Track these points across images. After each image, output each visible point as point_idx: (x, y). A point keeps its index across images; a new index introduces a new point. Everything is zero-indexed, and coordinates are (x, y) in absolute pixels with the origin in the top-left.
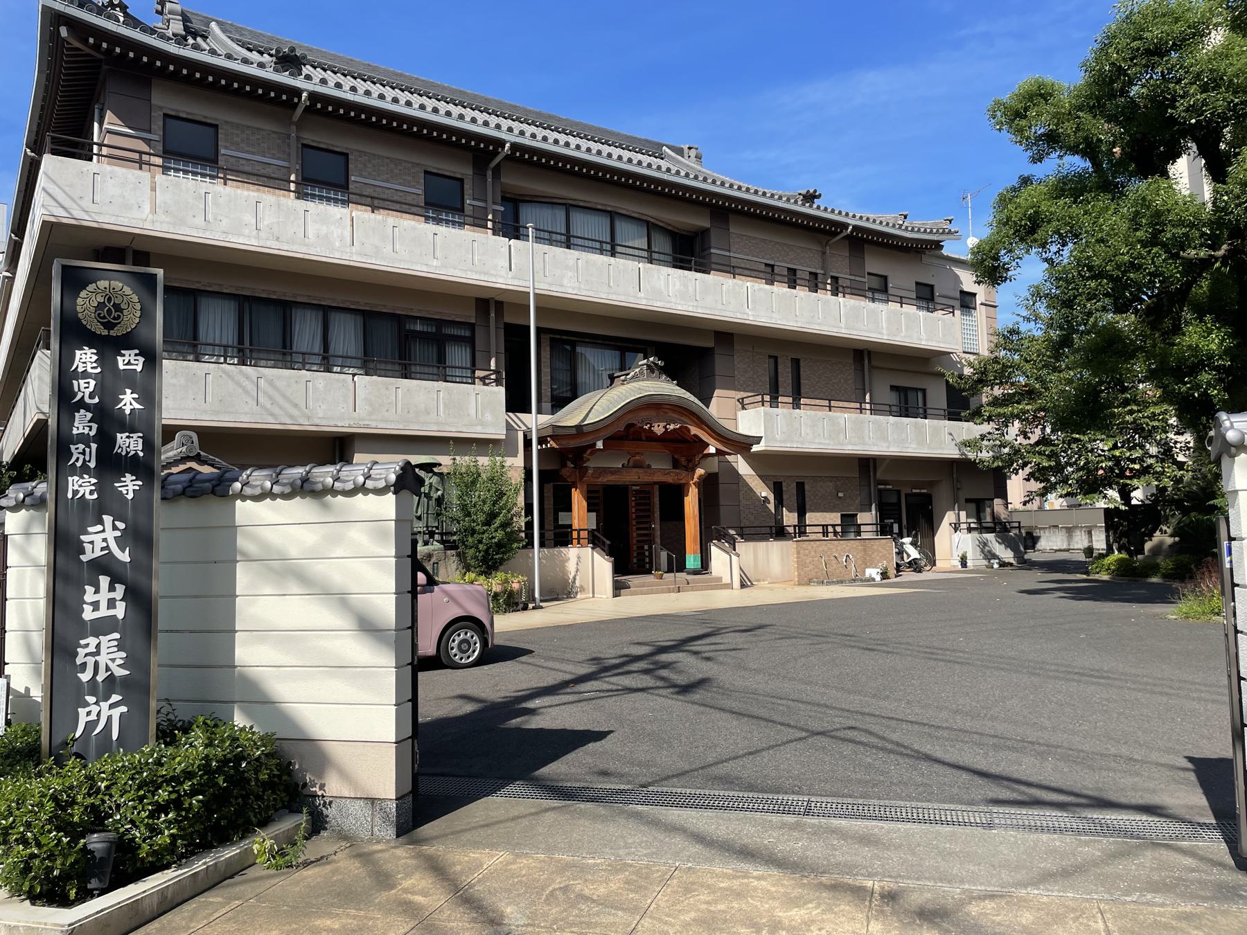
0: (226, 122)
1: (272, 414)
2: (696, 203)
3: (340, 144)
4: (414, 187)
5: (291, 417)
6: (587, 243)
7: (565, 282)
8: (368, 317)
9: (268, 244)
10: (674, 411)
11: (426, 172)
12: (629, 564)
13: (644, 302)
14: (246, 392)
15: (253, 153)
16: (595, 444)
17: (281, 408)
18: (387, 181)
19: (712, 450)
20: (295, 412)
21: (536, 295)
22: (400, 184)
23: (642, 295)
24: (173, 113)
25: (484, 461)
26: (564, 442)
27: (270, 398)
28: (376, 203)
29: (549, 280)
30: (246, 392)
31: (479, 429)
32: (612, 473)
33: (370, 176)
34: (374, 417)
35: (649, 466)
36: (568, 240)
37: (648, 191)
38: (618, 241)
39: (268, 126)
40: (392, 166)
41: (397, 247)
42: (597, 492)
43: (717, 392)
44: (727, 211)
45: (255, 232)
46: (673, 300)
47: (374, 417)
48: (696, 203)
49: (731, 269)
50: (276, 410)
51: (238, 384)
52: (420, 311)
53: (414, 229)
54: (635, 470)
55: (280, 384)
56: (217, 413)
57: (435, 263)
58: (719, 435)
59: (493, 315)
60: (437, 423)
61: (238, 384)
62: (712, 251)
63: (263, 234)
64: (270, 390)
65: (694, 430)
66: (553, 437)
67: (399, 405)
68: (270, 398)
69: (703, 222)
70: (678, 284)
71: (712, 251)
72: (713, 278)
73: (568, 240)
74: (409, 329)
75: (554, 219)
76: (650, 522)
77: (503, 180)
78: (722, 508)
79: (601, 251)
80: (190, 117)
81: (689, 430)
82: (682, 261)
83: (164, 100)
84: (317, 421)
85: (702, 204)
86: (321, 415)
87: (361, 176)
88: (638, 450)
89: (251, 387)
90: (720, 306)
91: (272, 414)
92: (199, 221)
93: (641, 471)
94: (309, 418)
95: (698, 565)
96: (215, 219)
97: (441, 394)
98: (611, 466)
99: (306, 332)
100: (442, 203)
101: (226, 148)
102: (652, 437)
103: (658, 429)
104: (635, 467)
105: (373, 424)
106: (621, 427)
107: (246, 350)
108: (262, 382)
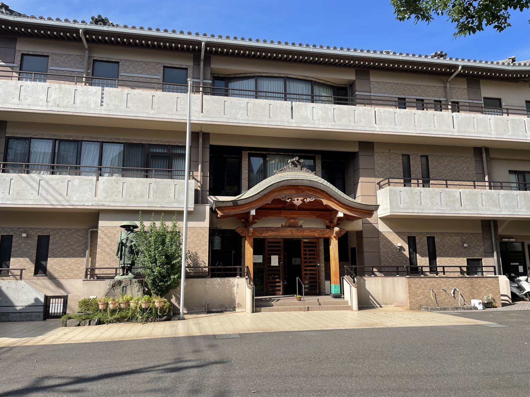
0: (53, 54)
1: (46, 200)
2: (345, 66)
3: (114, 57)
4: (157, 75)
5: (57, 200)
6: (274, 95)
7: (239, 116)
8: (128, 146)
9: (53, 109)
10: (309, 190)
11: (164, 67)
12: (265, 288)
13: (295, 125)
14: (33, 188)
15: (66, 67)
16: (249, 212)
17: (52, 196)
18: (141, 74)
19: (340, 215)
20: (60, 198)
21: (192, 125)
22: (149, 74)
23: (294, 120)
24: (26, 53)
25: (169, 224)
26: (226, 211)
27: (46, 190)
28: (134, 84)
29: (228, 116)
30: (33, 188)
31: (176, 205)
32: (272, 231)
33: (131, 72)
34: (107, 200)
35: (301, 226)
36: (285, 96)
37: (316, 63)
38: (288, 92)
39: (75, 53)
40: (144, 65)
41: (129, 105)
42: (280, 243)
43: (361, 179)
44: (365, 68)
45: (46, 103)
46: (317, 122)
47: (107, 200)
48: (345, 66)
49: (368, 101)
50: (49, 197)
51: (29, 184)
52: (135, 140)
53: (140, 94)
54: (290, 229)
55: (52, 183)
56: (15, 200)
57: (152, 111)
58: (344, 204)
59: (201, 140)
60: (148, 202)
61: (29, 184)
62: (356, 93)
63: (50, 104)
64: (46, 186)
65: (325, 202)
66: (220, 208)
67: (124, 192)
68: (46, 190)
69: (348, 77)
70: (320, 112)
71: (356, 93)
72: (360, 109)
73: (285, 96)
74: (148, 151)
75: (277, 86)
76: (315, 262)
77: (212, 66)
78: (365, 254)
79: (307, 100)
80: (35, 53)
81: (321, 203)
82: (338, 99)
83: (22, 47)
84: (73, 203)
85: (349, 66)
86: (75, 199)
87: (125, 72)
88: (292, 216)
89: (36, 185)
90: (352, 124)
91: (46, 200)
92: (16, 100)
93: (294, 229)
94: (68, 201)
95: (338, 291)
96: (25, 99)
97: (152, 185)
98: (275, 227)
99: (90, 154)
100: (172, 81)
101: (52, 66)
102: (292, 207)
103: (298, 202)
104: (289, 227)
105: (107, 204)
106: (269, 200)
107: (55, 166)
108: (42, 182)
